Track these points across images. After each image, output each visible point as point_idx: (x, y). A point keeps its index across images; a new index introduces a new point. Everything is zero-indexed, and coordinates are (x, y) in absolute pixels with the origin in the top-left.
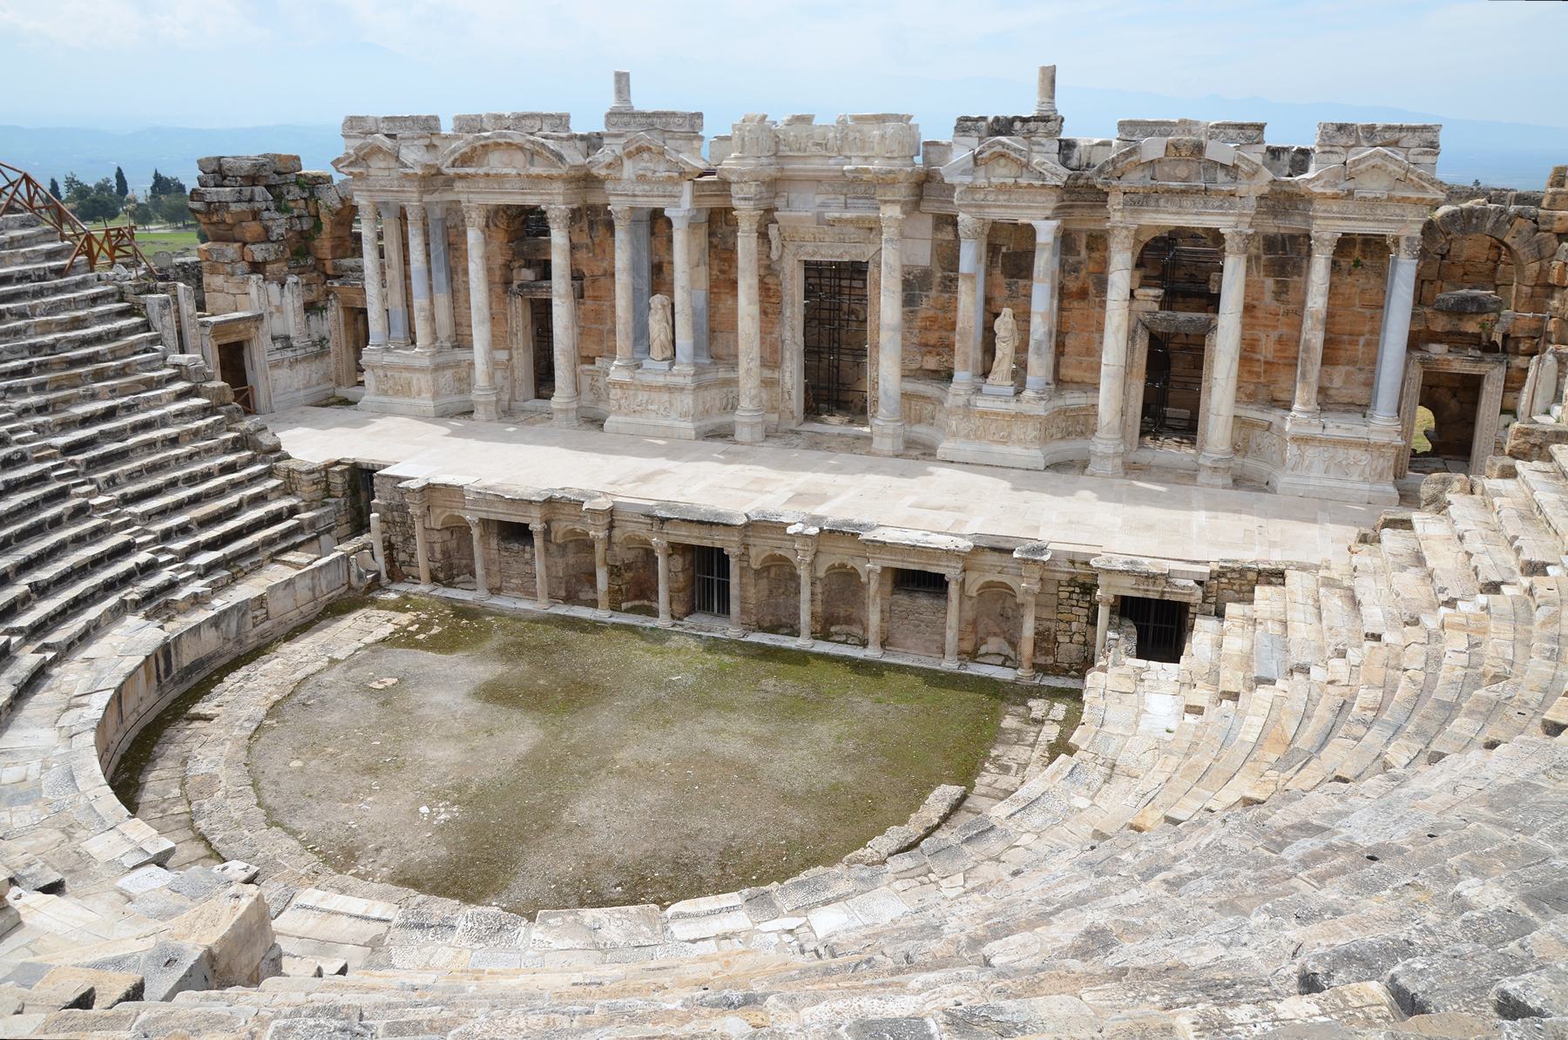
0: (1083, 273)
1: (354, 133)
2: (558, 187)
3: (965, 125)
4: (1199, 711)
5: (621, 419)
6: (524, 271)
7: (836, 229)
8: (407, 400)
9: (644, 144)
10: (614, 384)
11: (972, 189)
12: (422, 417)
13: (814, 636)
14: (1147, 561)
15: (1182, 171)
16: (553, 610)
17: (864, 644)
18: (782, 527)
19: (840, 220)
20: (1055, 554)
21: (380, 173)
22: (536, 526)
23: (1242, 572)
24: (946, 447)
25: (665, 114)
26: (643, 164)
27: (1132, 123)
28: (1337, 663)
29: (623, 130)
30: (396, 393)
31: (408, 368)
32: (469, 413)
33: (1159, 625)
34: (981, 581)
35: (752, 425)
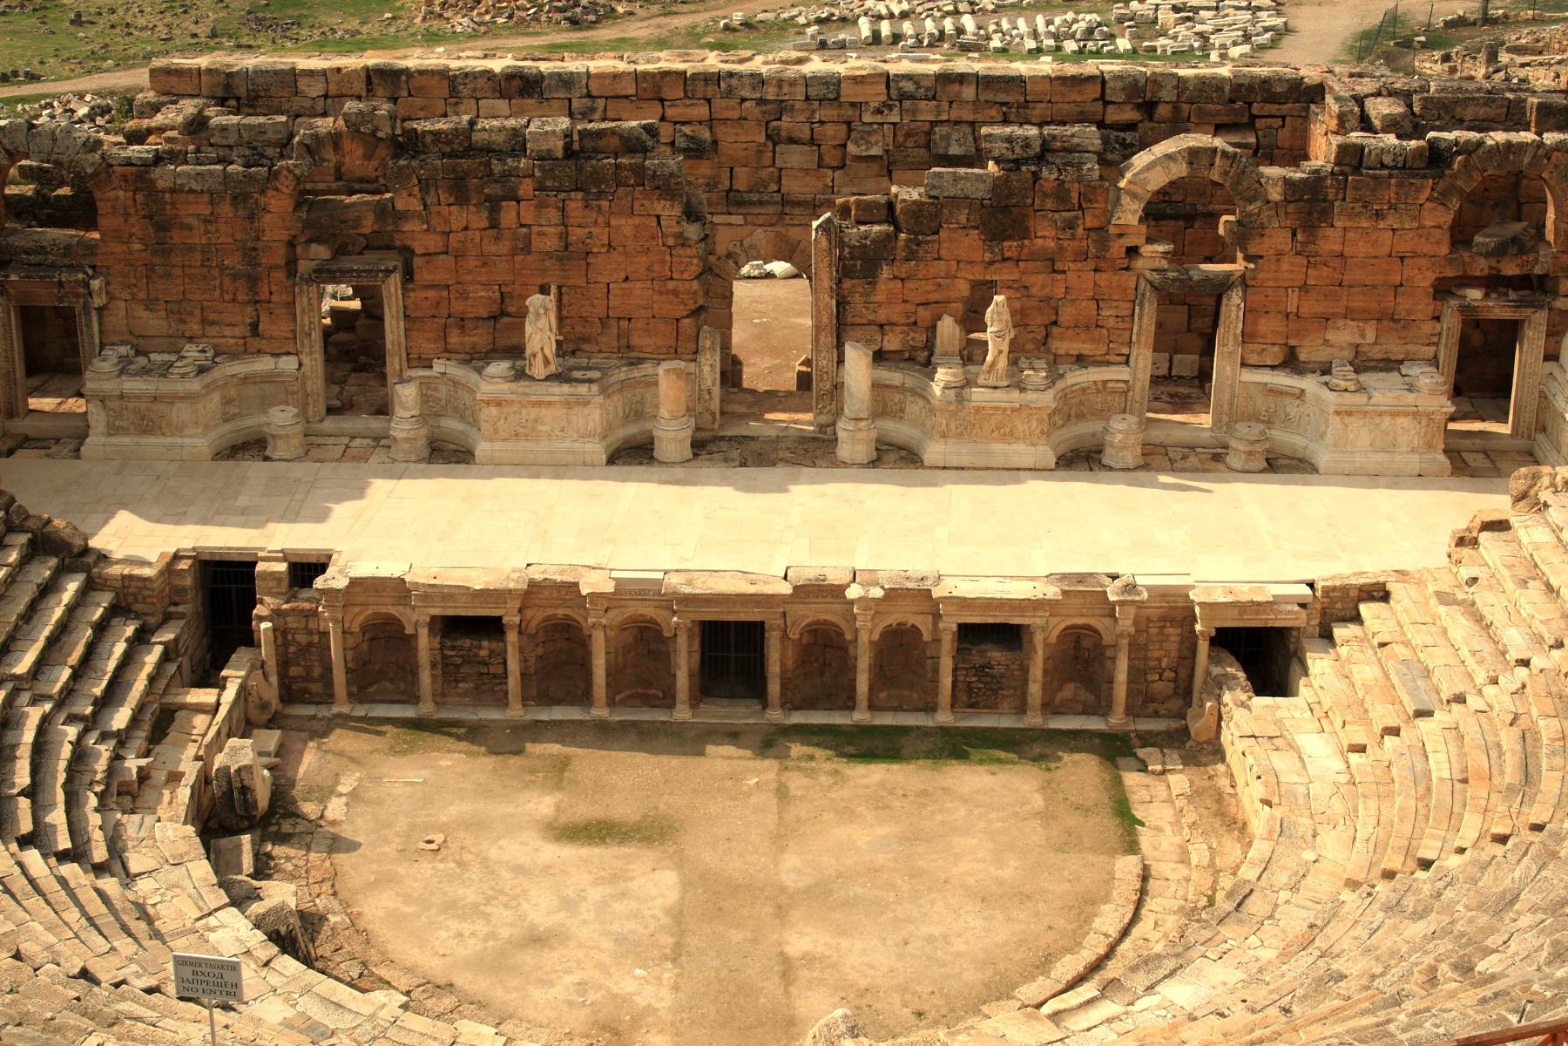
0: (1080, 231)
4: (1361, 749)
5: (498, 445)
6: (314, 247)
13: (872, 707)
14: (1246, 587)
16: (528, 717)
17: (930, 708)
18: (839, 591)
20: (1149, 588)
22: (511, 619)
23: (1345, 589)
24: (933, 451)
28: (1490, 691)
32: (253, 446)
33: (1265, 653)
34: (1062, 626)
35: (681, 441)
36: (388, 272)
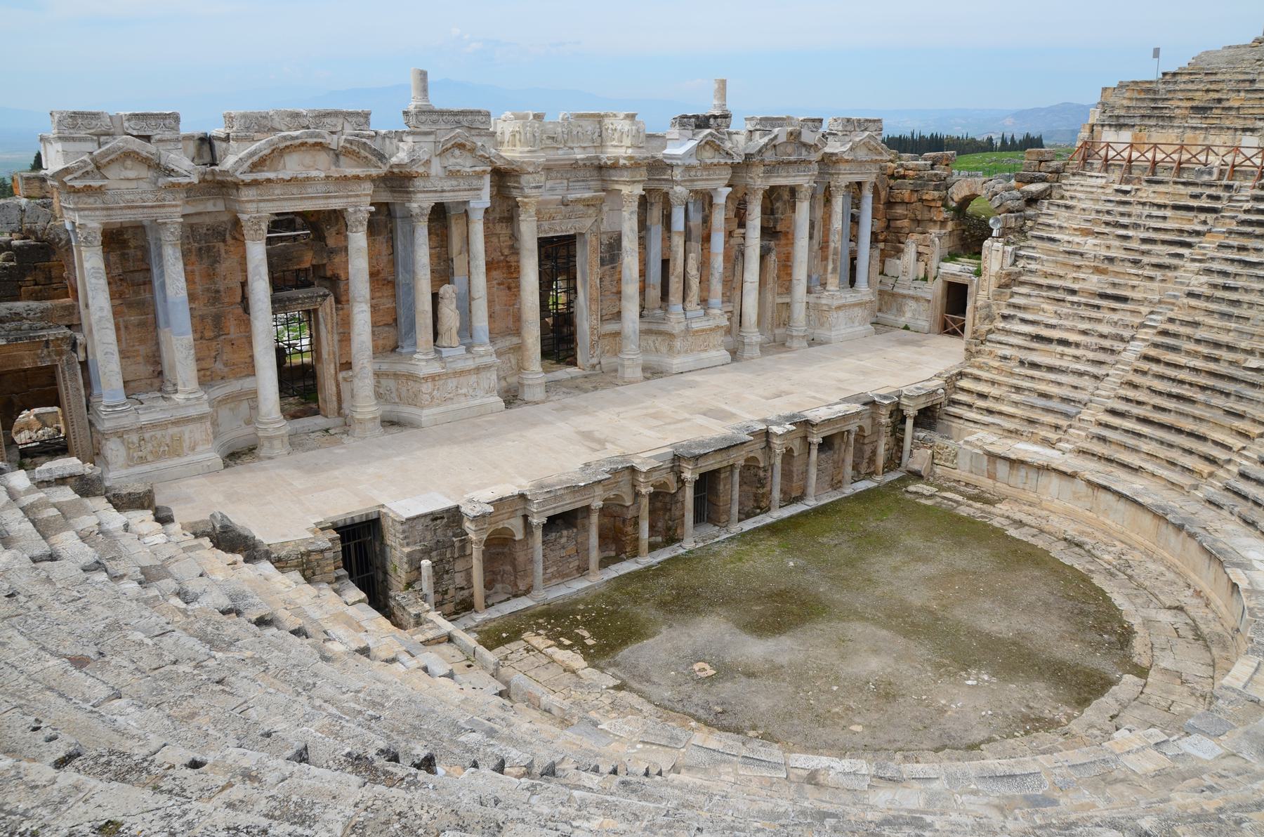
1: (82, 134)
2: (368, 188)
3: (683, 121)
7: (569, 208)
8: (176, 461)
9: (459, 140)
10: (425, 379)
11: (688, 168)
12: (209, 472)
15: (789, 149)
19: (578, 201)
21: (124, 185)
25: (472, 112)
26: (452, 161)
27: (766, 119)
29: (434, 128)
30: (159, 456)
31: (176, 423)
36: (325, 296)
